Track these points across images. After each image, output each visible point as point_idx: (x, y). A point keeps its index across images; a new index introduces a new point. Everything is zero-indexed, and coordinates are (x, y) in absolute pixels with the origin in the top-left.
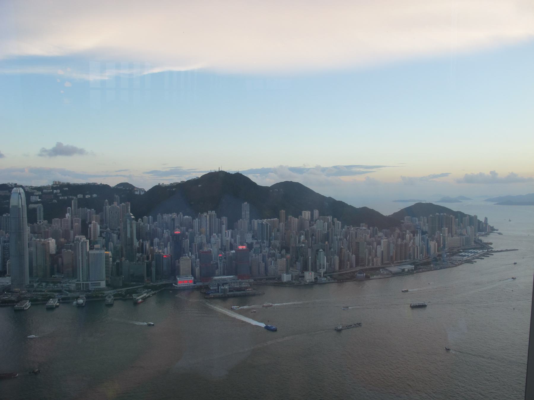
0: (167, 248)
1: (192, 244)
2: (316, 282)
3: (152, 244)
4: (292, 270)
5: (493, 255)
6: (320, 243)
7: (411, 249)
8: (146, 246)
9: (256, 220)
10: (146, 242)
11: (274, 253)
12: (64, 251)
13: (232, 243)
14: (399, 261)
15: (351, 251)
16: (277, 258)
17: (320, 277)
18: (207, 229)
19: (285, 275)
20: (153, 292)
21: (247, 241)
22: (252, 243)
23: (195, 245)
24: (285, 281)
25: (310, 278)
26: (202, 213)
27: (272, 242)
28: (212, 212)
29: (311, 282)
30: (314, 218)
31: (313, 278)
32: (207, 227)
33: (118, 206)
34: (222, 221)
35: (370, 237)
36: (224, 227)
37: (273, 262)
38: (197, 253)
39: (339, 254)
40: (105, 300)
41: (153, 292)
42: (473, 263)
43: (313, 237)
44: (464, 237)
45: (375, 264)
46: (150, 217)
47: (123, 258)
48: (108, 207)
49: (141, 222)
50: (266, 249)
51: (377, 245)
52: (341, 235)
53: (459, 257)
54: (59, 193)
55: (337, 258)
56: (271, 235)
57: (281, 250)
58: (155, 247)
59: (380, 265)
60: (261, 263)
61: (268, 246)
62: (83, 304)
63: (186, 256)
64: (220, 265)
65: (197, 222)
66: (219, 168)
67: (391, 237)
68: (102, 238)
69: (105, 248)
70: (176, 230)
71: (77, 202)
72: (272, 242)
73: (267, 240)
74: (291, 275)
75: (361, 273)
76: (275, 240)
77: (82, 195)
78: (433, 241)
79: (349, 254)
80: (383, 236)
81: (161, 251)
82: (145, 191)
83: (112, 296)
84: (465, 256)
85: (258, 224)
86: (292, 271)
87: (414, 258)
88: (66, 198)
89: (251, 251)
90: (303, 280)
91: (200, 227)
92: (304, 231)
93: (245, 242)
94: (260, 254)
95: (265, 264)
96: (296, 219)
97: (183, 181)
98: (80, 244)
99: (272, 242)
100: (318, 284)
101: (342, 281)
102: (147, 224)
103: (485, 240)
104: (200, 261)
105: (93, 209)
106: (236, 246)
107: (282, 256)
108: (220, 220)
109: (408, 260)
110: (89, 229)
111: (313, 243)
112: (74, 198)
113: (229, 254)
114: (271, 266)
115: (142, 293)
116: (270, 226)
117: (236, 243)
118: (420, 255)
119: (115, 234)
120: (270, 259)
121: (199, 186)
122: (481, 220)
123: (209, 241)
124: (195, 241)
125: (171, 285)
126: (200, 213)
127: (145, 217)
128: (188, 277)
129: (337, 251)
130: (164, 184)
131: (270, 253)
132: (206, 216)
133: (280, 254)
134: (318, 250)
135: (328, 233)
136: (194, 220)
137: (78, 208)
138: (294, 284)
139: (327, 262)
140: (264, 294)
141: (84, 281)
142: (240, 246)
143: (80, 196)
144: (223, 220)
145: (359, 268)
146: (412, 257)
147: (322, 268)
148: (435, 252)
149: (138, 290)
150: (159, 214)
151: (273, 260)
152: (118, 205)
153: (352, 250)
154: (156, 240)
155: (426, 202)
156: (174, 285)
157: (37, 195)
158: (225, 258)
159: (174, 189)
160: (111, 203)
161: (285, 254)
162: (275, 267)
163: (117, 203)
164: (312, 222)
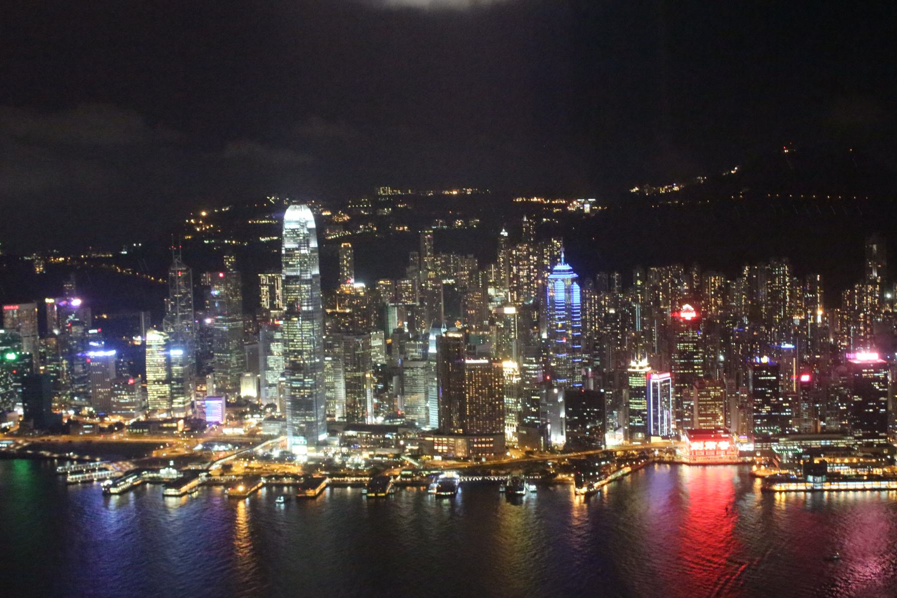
41: (628, 469)
68: (496, 327)
83: (523, 474)
105: (471, 253)
113: (830, 375)
125: (672, 451)
137: (436, 253)
141: (452, 435)
143: (440, 224)
156: (678, 451)
157: (337, 224)
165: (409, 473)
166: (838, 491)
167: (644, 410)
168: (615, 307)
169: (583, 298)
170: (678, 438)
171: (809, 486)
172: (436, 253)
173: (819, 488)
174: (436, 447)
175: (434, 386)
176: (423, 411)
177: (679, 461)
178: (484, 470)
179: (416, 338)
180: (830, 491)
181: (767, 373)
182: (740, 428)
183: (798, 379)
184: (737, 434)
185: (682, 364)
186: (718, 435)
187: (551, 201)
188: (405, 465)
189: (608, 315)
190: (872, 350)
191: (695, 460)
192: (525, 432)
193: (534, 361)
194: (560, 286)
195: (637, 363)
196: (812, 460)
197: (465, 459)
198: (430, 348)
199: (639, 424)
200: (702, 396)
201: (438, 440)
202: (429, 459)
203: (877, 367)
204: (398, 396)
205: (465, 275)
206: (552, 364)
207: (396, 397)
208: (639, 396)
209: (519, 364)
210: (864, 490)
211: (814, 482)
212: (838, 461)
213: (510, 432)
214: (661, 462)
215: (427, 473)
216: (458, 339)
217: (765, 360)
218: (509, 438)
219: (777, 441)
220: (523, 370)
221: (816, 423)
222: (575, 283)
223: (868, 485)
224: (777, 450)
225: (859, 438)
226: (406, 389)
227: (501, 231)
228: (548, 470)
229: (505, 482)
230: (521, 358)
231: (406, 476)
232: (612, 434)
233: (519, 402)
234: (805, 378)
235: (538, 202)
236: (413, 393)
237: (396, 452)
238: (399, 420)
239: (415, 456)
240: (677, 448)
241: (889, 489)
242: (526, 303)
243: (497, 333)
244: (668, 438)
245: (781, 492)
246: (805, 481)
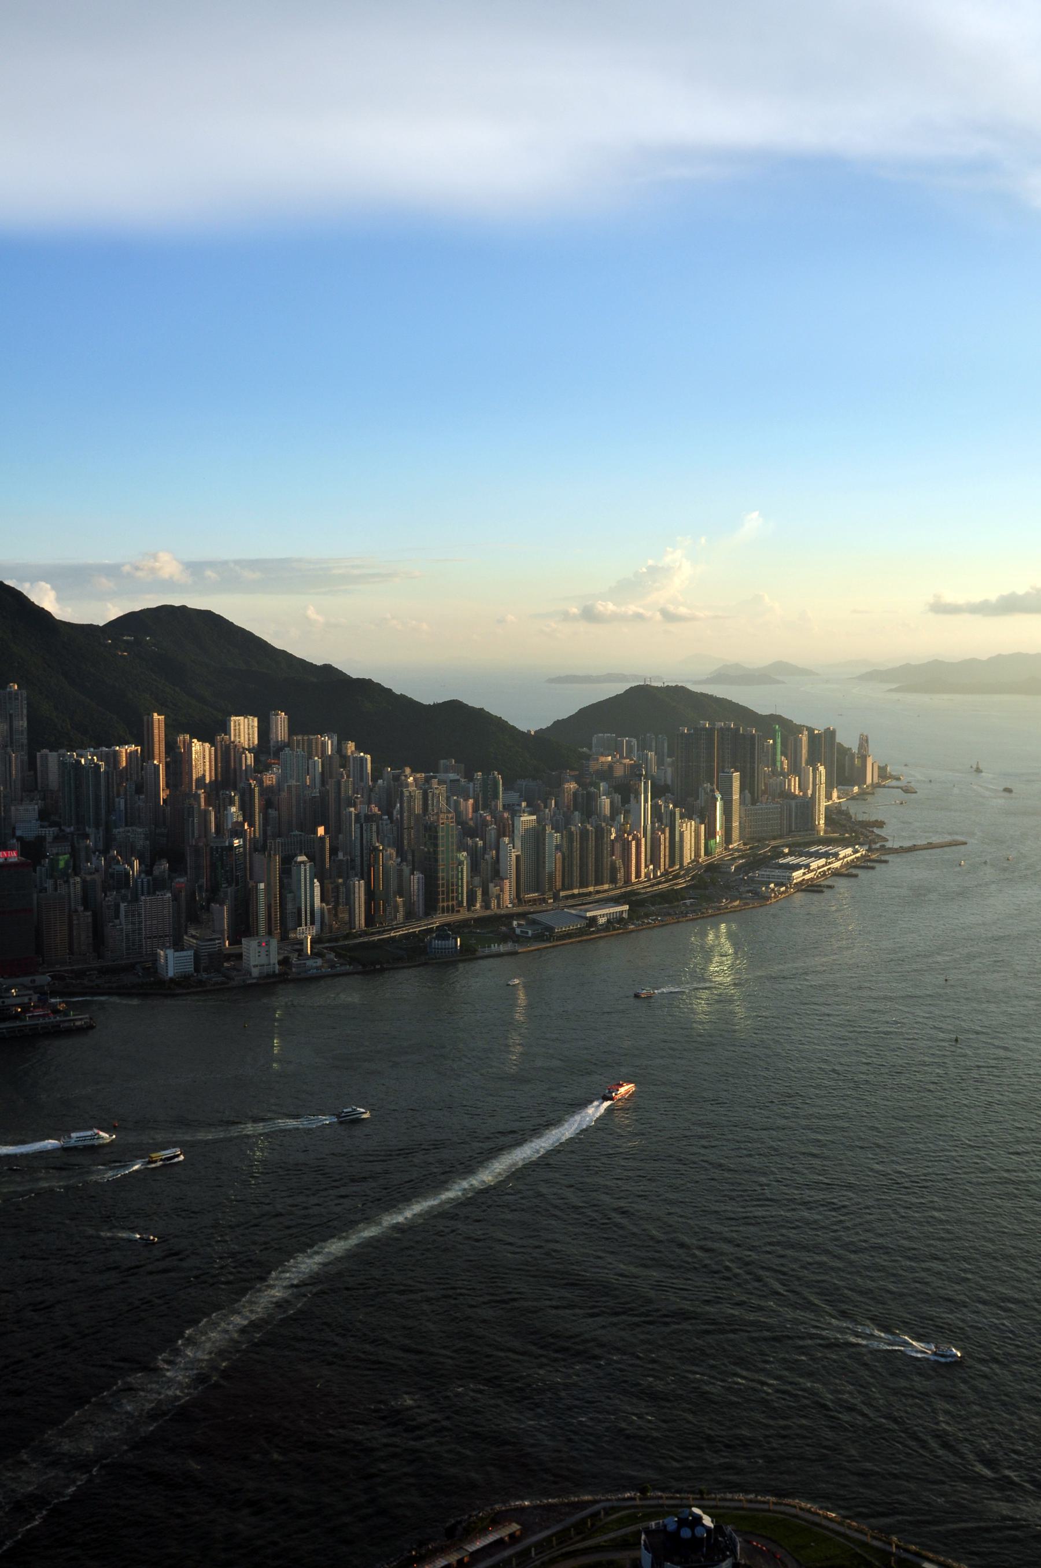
2: (287, 974)
4: (194, 933)
5: (886, 862)
6: (297, 833)
7: (618, 846)
14: (576, 891)
15: (410, 857)
16: (140, 892)
17: (299, 955)
19: (170, 952)
21: (18, 833)
22: (41, 839)
24: (171, 974)
25: (263, 960)
27: (115, 831)
29: (268, 976)
30: (272, 743)
31: (274, 959)
35: (476, 809)
37: (123, 906)
39: (366, 869)
42: (822, 892)
43: (270, 811)
44: (793, 803)
45: (494, 903)
50: (94, 859)
51: (501, 833)
52: (369, 803)
53: (777, 872)
55: (359, 887)
56: (111, 809)
57: (152, 864)
59: (510, 906)
60: (76, 911)
61: (101, 847)
67: (546, 807)
72: (115, 831)
73: (97, 826)
74: (191, 953)
75: (446, 937)
76: (126, 825)
78: (690, 818)
79: (400, 872)
80: (520, 805)
84: (797, 867)
85: (63, 765)
86: (193, 937)
87: (627, 881)
89: (38, 868)
90: (239, 970)
92: (235, 789)
93: (14, 835)
94: (72, 881)
95: (95, 915)
96: (207, 745)
99: (119, 831)
100: (295, 981)
101: (378, 967)
103: (859, 812)
107: (157, 885)
109: (606, 887)
111: (269, 833)
114: (117, 921)
118: (646, 866)
120: (112, 897)
122: (846, 745)
129: (358, 860)
131: (112, 876)
133: (150, 878)
134: (288, 861)
135: (324, 795)
138: (201, 983)
139: (322, 900)
140: (91, 1027)
145: (437, 921)
146: (621, 875)
147: (306, 925)
148: (697, 855)
151: (124, 899)
153: (413, 856)
155: (666, 685)
161: (169, 875)
162: (130, 926)
164: (263, 758)
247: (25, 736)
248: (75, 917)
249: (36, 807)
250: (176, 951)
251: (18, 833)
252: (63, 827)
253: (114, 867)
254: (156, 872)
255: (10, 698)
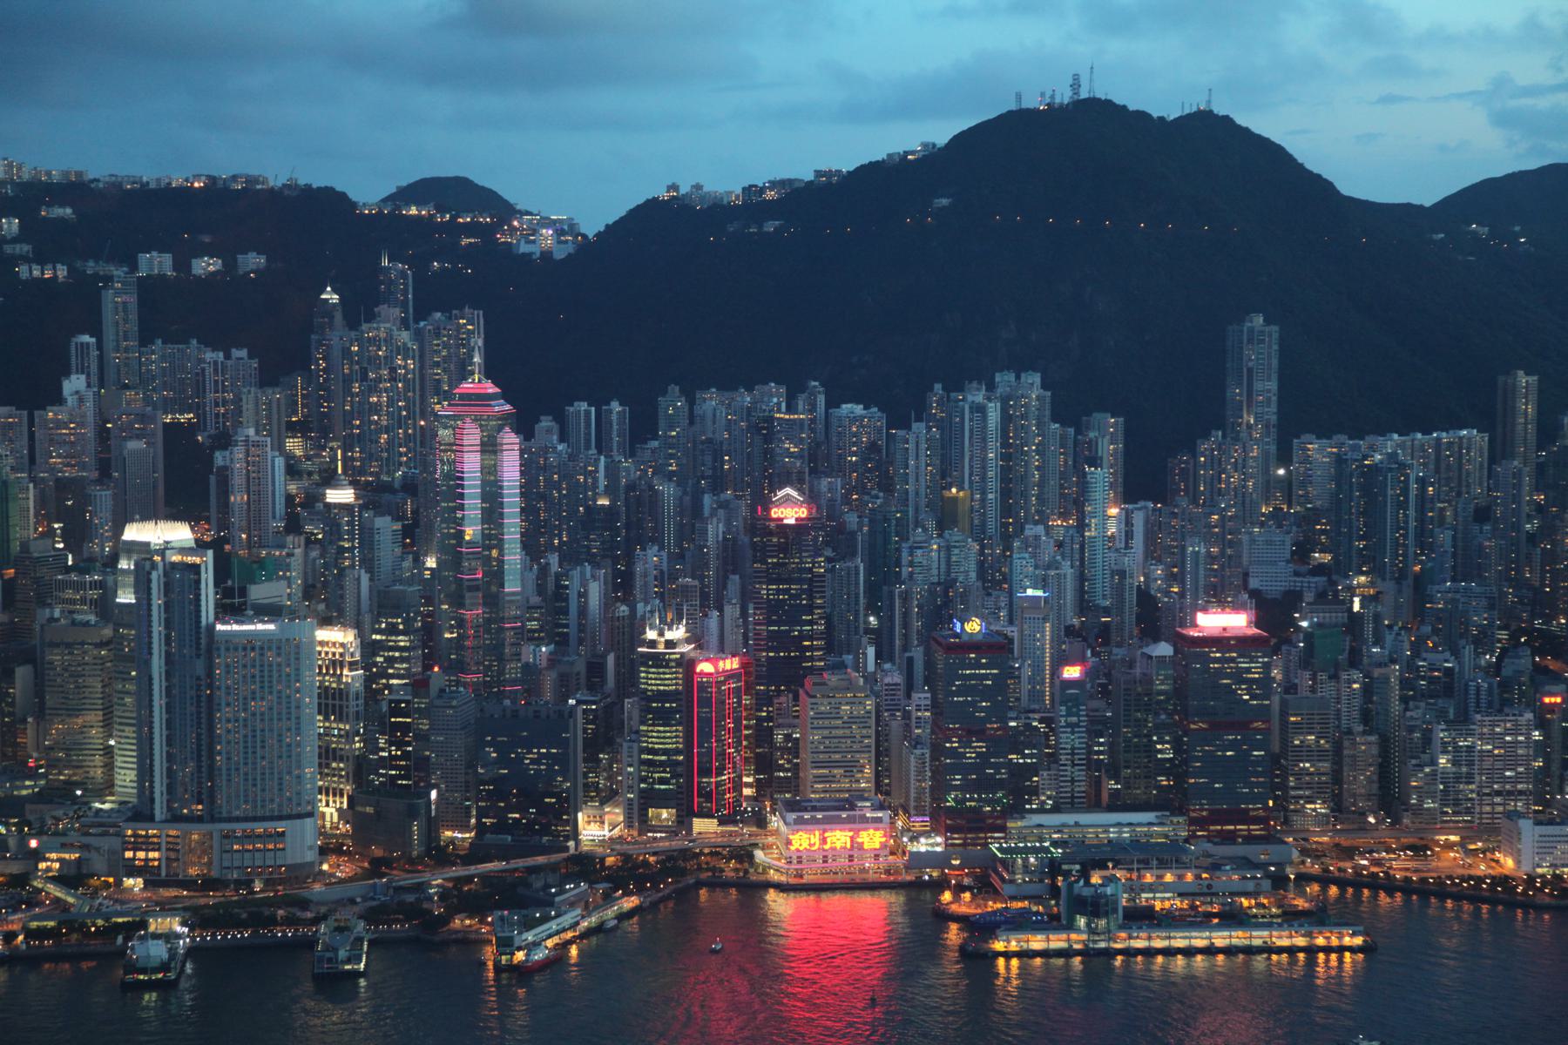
0: (721, 610)
1: (885, 588)
3: (622, 585)
8: (583, 595)
9: (1318, 437)
10: (583, 574)
11: (1448, 672)
12: (52, 620)
13: (1153, 592)
18: (984, 493)
19: (1525, 825)
20: (630, 903)
21: (1254, 583)
22: (1292, 600)
23: (906, 597)
26: (955, 384)
28: (1018, 377)
32: (984, 478)
33: (404, 336)
34: (1092, 445)
36: (1101, 477)
38: (918, 653)
40: (310, 943)
41: (630, 903)
46: (616, 407)
47: (436, 669)
48: (337, 336)
49: (555, 437)
50: (1389, 638)
54: (15, 240)
58: (640, 606)
60: (1350, 732)
62: (164, 967)
63: (841, 666)
64: (1070, 740)
65: (924, 446)
66: (1076, 85)
68: (302, 538)
69: (322, 607)
70: (780, 494)
71: (132, 299)
72: (1432, 589)
77: (167, 259)
81: (678, 633)
82: (584, 236)
83: (360, 917)
85: (1339, 460)
88: (62, 271)
89: (1284, 648)
91: (946, 471)
94: (1344, 675)
95: (1384, 743)
97: (828, 174)
98: (154, 575)
102: (593, 451)
104: (935, 706)
105: (239, 346)
106: (1181, 609)
108: (1078, 432)
110: (213, 479)
112: (119, 272)
113: (1131, 664)
114: (1425, 757)
115: (551, 904)
116: (1423, 483)
117: (1182, 595)
119: (382, 515)
120: (1417, 713)
121: (944, 202)
123: (995, 578)
124: (906, 571)
125: (744, 855)
126: (938, 387)
127: (584, 406)
128: (853, 807)
130: (705, 189)
132: (980, 410)
136: (901, 433)
137: (145, 340)
141: (175, 818)
142: (1205, 610)
143: (156, 263)
144: (1092, 435)
149: (528, 885)
150: (674, 389)
151: (1441, 715)
152: (405, 324)
154: (651, 559)
156: (759, 855)
158: (1105, 692)
159: (770, 227)
160: (359, 310)
163: (396, 312)
165: (52, 924)
166: (1149, 953)
167: (677, 752)
168: (609, 491)
169: (527, 468)
170: (761, 822)
171: (1077, 940)
172: (145, 340)
173: (1103, 945)
174: (129, 854)
175: (128, 693)
176: (98, 759)
177: (762, 878)
178: (259, 916)
179: (84, 566)
180: (1129, 953)
181: (977, 660)
182: (913, 795)
183: (1055, 672)
184: (906, 811)
185: (772, 636)
186: (858, 813)
187: (453, 218)
188: (40, 904)
189: (592, 510)
190: (1237, 608)
191: (801, 877)
192: (369, 810)
193: (401, 627)
194: (472, 436)
195: (661, 634)
196: (1084, 873)
197: (209, 884)
198: (120, 592)
199: (663, 787)
200: (820, 716)
201: (135, 835)
202: (107, 885)
203: (1243, 644)
204: (30, 720)
205: (225, 402)
206: (447, 635)
207: (24, 721)
208: (664, 718)
209: (361, 635)
210: (1210, 951)
211: (1092, 931)
212: (1149, 878)
213: (329, 810)
214: (718, 884)
215: (100, 922)
216: (195, 568)
217: (974, 626)
218: (328, 825)
219: (1003, 829)
220: (369, 649)
221: (1097, 784)
222: (507, 429)
223: (1221, 939)
224: (1000, 849)
225: (1201, 823)
226: (50, 701)
227: (323, 291)
228: (426, 905)
229: (310, 943)
230: (367, 618)
231: (41, 934)
232: (591, 812)
233: (358, 734)
234: (1072, 672)
235: (418, 218)
236: (75, 711)
237: (15, 868)
238: (27, 783)
239: (70, 878)
240: (755, 845)
241: (1269, 950)
242: (385, 478)
243: (306, 554)
244: (735, 822)
245: (1007, 955)
246: (1070, 927)
247: (1274, 408)
248: (1346, 743)
249: (1288, 539)
250: (1538, 823)
251: (1254, 583)
252: (1335, 577)
253: (1424, 655)
254: (1507, 671)
255: (1250, 341)
